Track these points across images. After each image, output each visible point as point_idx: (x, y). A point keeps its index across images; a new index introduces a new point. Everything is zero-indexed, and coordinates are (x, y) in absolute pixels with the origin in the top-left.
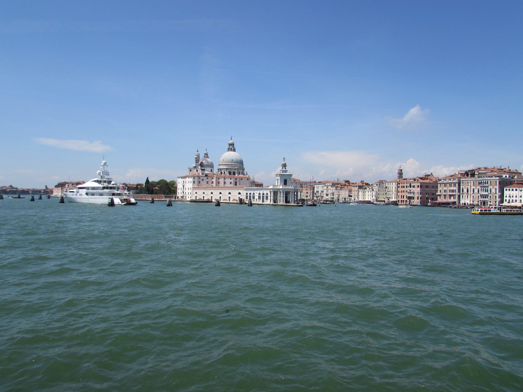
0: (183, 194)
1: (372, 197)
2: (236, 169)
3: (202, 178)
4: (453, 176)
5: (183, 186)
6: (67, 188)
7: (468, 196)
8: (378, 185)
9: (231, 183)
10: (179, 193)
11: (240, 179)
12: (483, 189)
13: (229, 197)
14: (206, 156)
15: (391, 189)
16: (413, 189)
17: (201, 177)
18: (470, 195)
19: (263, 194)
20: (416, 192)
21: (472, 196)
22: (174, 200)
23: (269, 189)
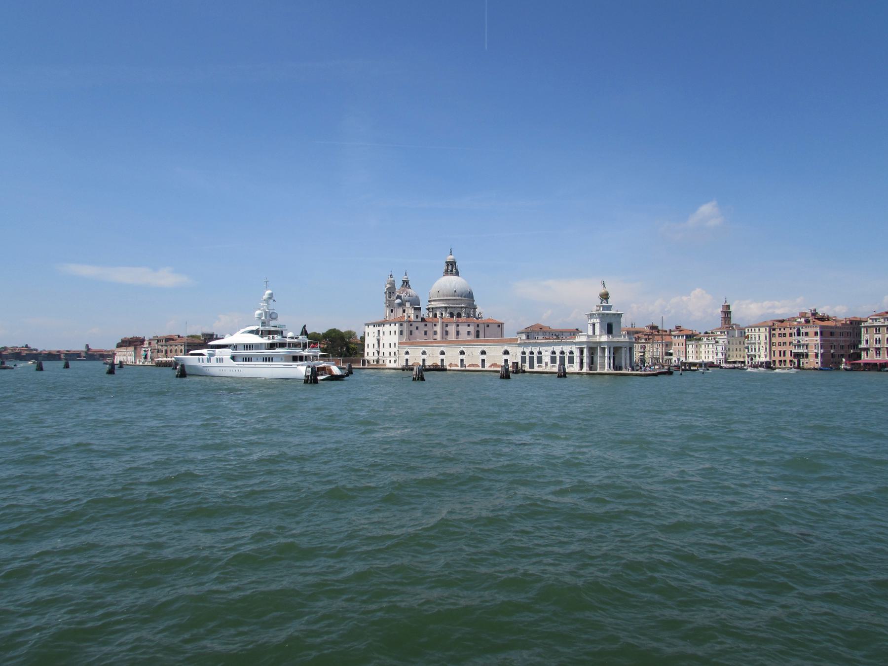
0: (379, 355)
2: (462, 308)
3: (415, 325)
5: (379, 341)
6: (147, 348)
8: (726, 333)
9: (469, 333)
10: (370, 353)
11: (486, 326)
14: (406, 283)
15: (757, 339)
16: (806, 339)
17: (413, 323)
19: (562, 353)
20: (811, 344)
22: (361, 366)
23: (575, 343)
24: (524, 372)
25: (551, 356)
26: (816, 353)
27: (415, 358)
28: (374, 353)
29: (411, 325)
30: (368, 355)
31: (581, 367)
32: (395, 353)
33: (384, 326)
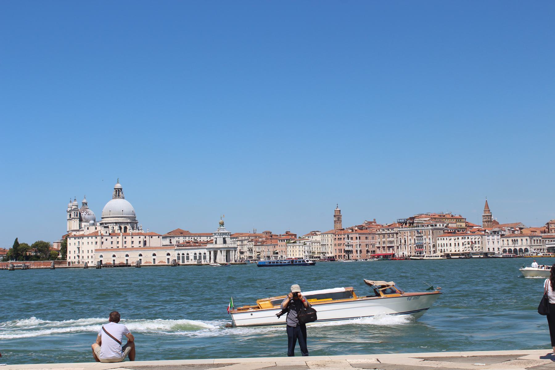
0: (79, 258)
1: (304, 253)
3: (105, 238)
4: (391, 226)
5: (79, 248)
7: (405, 247)
12: (419, 239)
16: (352, 242)
17: (104, 237)
18: (408, 246)
20: (354, 244)
21: (409, 247)
22: (67, 266)
24: (179, 265)
25: (194, 256)
26: (356, 250)
27: (108, 259)
28: (75, 257)
29: (102, 238)
30: (70, 258)
31: (210, 261)
32: (92, 256)
33: (83, 239)
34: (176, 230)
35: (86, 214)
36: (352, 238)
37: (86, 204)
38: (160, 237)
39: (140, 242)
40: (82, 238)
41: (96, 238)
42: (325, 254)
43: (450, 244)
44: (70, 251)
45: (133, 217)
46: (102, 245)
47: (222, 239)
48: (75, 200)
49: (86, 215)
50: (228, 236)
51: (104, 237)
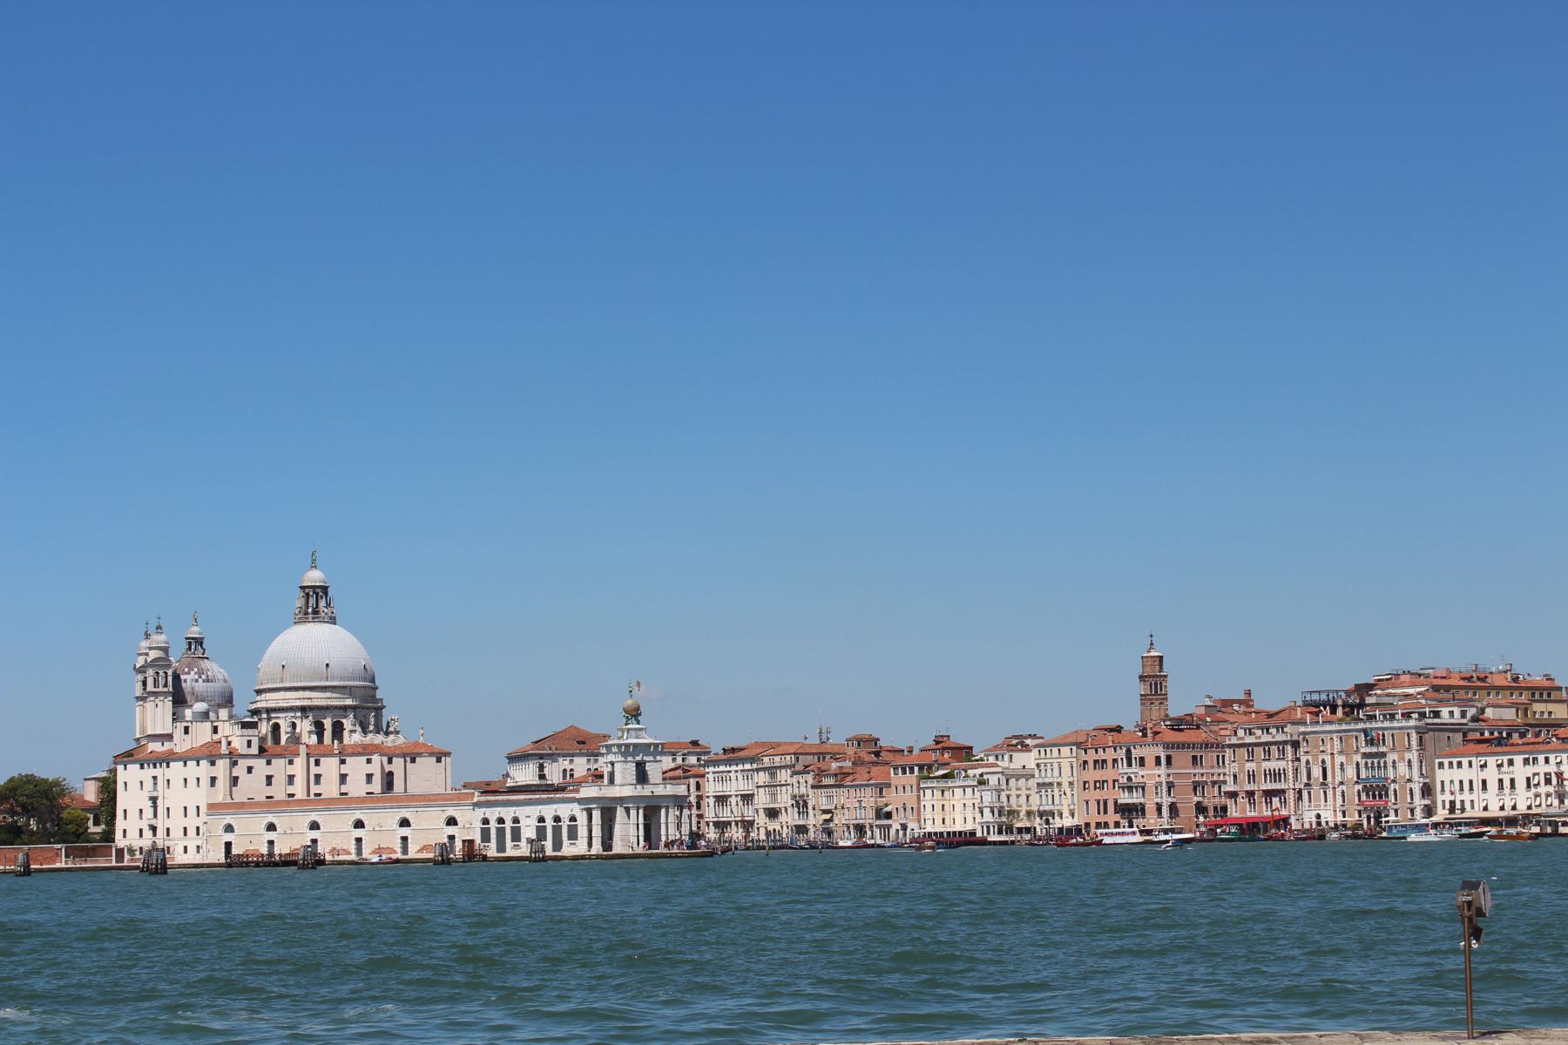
0: (155, 835)
1: (978, 816)
4: (1275, 718)
5: (154, 800)
7: (1325, 793)
12: (1373, 763)
13: (359, 840)
16: (1141, 773)
17: (240, 761)
18: (1334, 788)
20: (1150, 783)
21: (1339, 793)
22: (114, 864)
24: (485, 858)
25: (537, 826)
26: (1157, 804)
27: (250, 838)
28: (141, 830)
30: (125, 836)
31: (590, 845)
32: (198, 828)
33: (168, 766)
34: (562, 732)
35: (197, 677)
36: (1142, 759)
37: (199, 642)
38: (443, 759)
39: (369, 777)
40: (164, 765)
41: (213, 763)
42: (1050, 818)
43: (1484, 782)
44: (125, 811)
45: (364, 687)
46: (233, 788)
47: (632, 768)
48: (157, 628)
49: (197, 681)
50: (654, 758)
51: (240, 761)
